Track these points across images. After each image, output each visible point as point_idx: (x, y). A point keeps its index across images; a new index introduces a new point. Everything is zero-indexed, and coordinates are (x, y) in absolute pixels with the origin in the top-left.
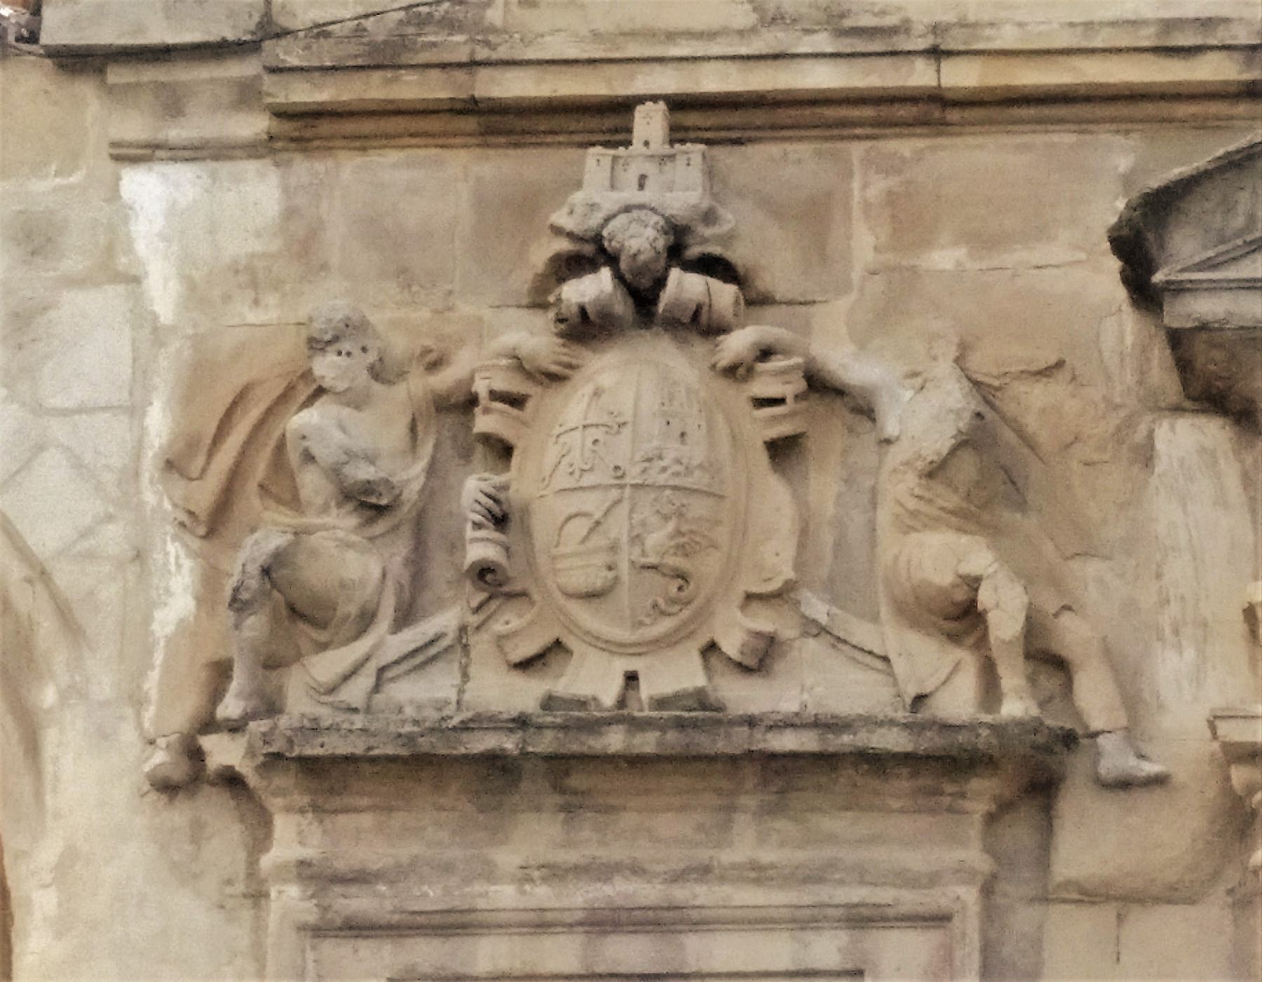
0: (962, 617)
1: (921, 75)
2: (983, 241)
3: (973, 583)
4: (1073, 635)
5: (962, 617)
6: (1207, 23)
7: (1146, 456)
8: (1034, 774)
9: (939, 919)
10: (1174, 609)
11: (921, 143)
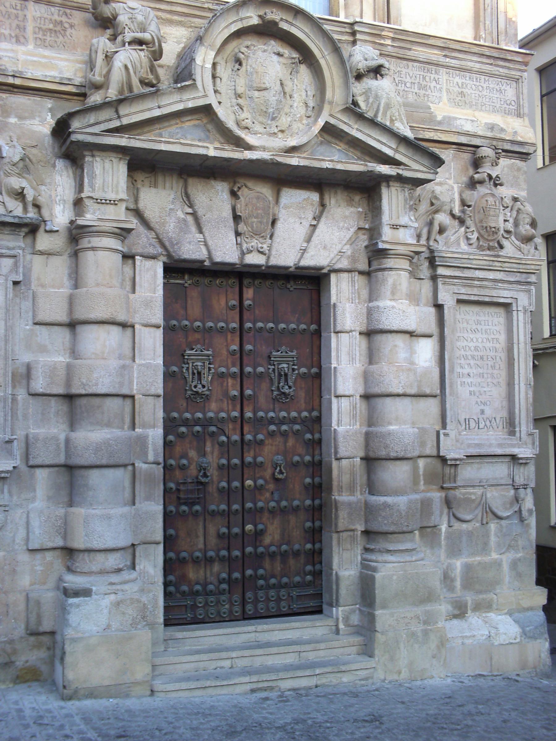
0: (20, 195)
1: (11, 80)
2: (21, 118)
3: (23, 189)
4: (42, 200)
5: (20, 195)
6: (69, 79)
7: (54, 166)
8: (32, 229)
9: (14, 256)
10: (59, 197)
11: (8, 95)
